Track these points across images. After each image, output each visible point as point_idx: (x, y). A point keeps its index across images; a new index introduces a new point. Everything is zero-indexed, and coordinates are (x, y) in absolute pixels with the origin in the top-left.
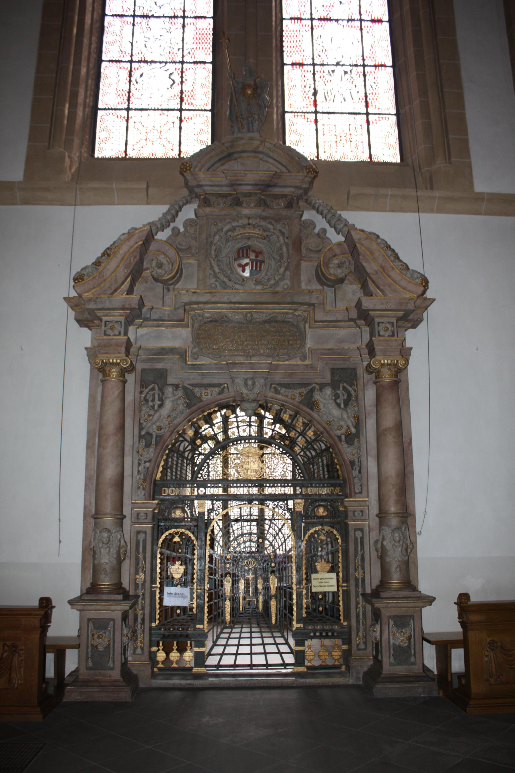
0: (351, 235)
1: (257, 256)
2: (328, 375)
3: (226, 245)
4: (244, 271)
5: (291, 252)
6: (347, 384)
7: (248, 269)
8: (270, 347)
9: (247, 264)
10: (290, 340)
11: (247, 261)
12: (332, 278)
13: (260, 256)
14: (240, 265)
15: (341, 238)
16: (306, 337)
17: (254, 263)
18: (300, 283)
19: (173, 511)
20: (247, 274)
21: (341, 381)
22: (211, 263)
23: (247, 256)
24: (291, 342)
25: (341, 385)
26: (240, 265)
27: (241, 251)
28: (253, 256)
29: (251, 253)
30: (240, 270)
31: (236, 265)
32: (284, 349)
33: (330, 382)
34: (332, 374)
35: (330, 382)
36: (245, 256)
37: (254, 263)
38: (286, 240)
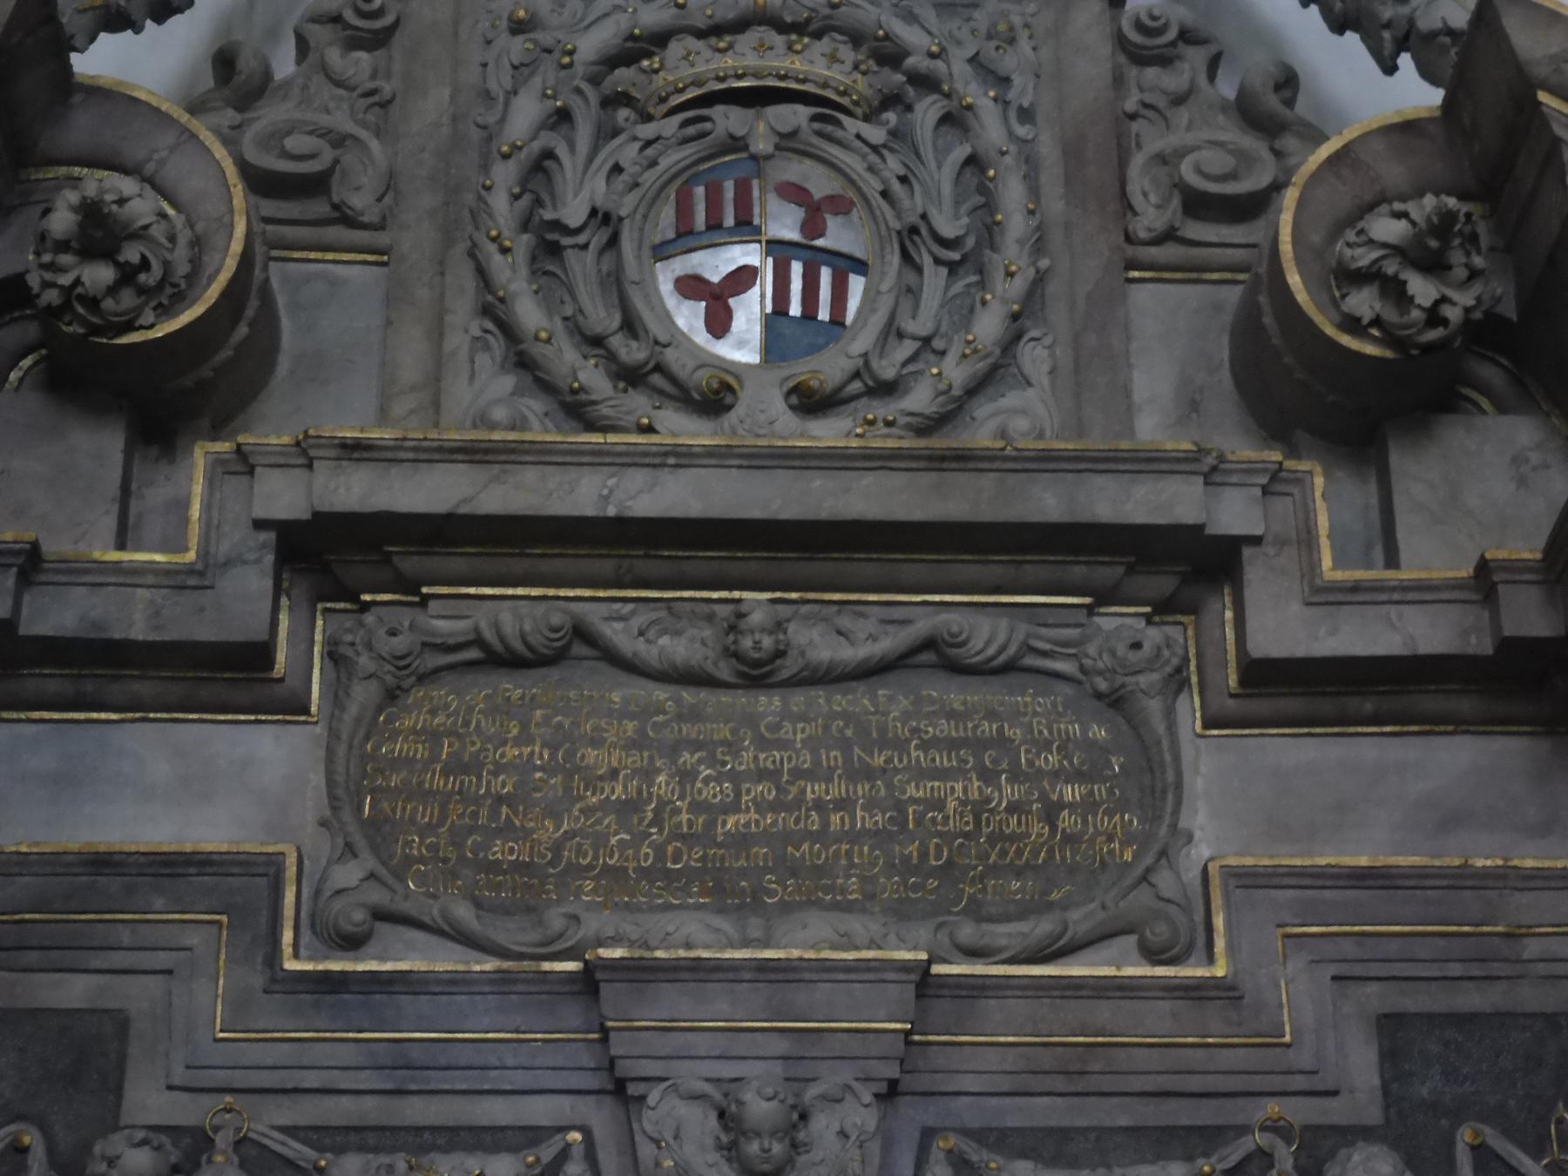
0: (1501, 38)
1: (813, 226)
2: (1361, 1065)
3: (590, 159)
4: (719, 323)
5: (1055, 204)
6: (1507, 1133)
7: (749, 311)
8: (913, 849)
9: (742, 278)
10: (1061, 805)
11: (747, 255)
12: (1370, 349)
13: (832, 223)
14: (691, 286)
15: (1413, 93)
16: (1179, 786)
17: (797, 269)
18: (1130, 411)
19: (205, 1157)
20: (742, 347)
21: (1458, 1115)
22: (482, 273)
23: (746, 228)
24: (1066, 820)
25: (1465, 1135)
26: (691, 286)
27: (700, 191)
28: (785, 224)
29: (774, 203)
30: (689, 317)
31: (666, 286)
32: (1019, 873)
33: (1373, 1115)
34: (1391, 1057)
35: (1373, 1115)
36: (729, 221)
37: (797, 269)
38: (1022, 131)
